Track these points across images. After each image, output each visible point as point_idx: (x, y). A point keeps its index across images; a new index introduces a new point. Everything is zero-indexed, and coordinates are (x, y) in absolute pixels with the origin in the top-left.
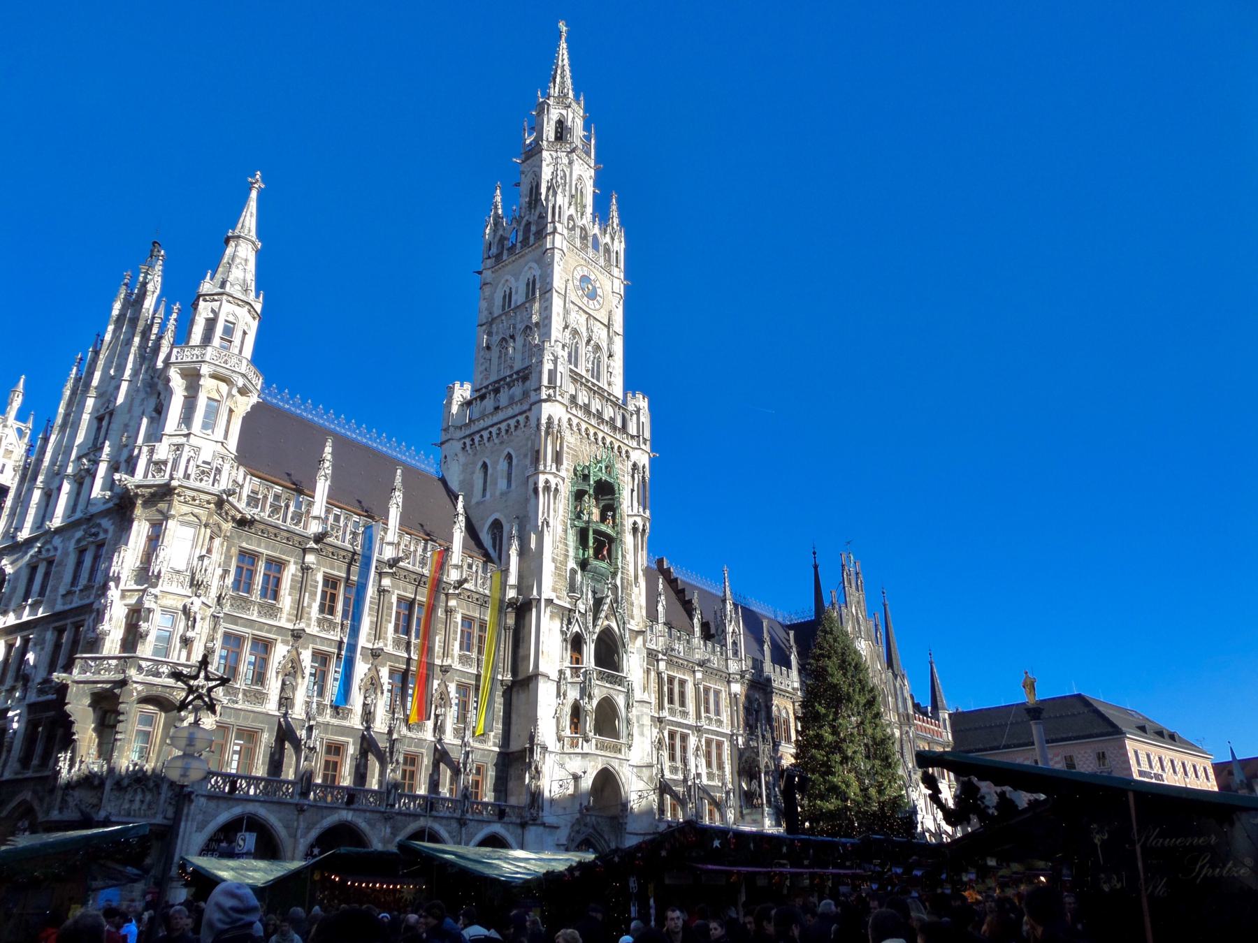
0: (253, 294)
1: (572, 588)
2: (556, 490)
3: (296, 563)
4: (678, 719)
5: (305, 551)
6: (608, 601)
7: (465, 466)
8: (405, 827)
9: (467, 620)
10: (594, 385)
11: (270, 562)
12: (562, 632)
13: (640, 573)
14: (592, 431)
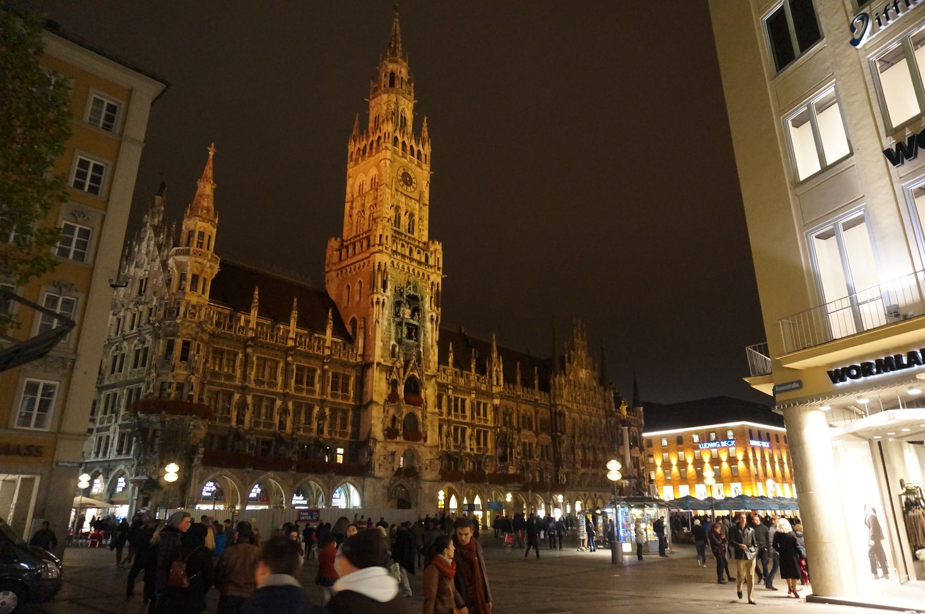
0: (212, 215)
1: (393, 354)
2: (383, 303)
4: (460, 420)
5: (246, 347)
7: (338, 286)
9: (335, 376)
10: (409, 238)
13: (435, 344)
14: (406, 267)
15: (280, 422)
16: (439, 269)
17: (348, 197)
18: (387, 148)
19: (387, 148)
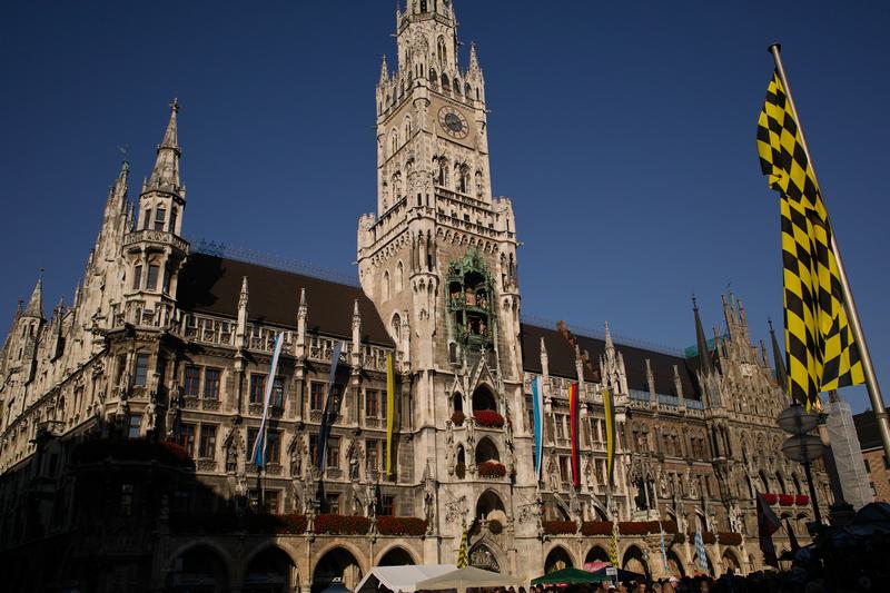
1: (453, 359)
2: (430, 286)
3: (229, 369)
6: (481, 364)
7: (375, 276)
8: (323, 546)
10: (464, 197)
11: (209, 370)
12: (448, 393)
15: (292, 463)
16: (510, 234)
17: (380, 162)
18: (419, 85)
19: (419, 85)
